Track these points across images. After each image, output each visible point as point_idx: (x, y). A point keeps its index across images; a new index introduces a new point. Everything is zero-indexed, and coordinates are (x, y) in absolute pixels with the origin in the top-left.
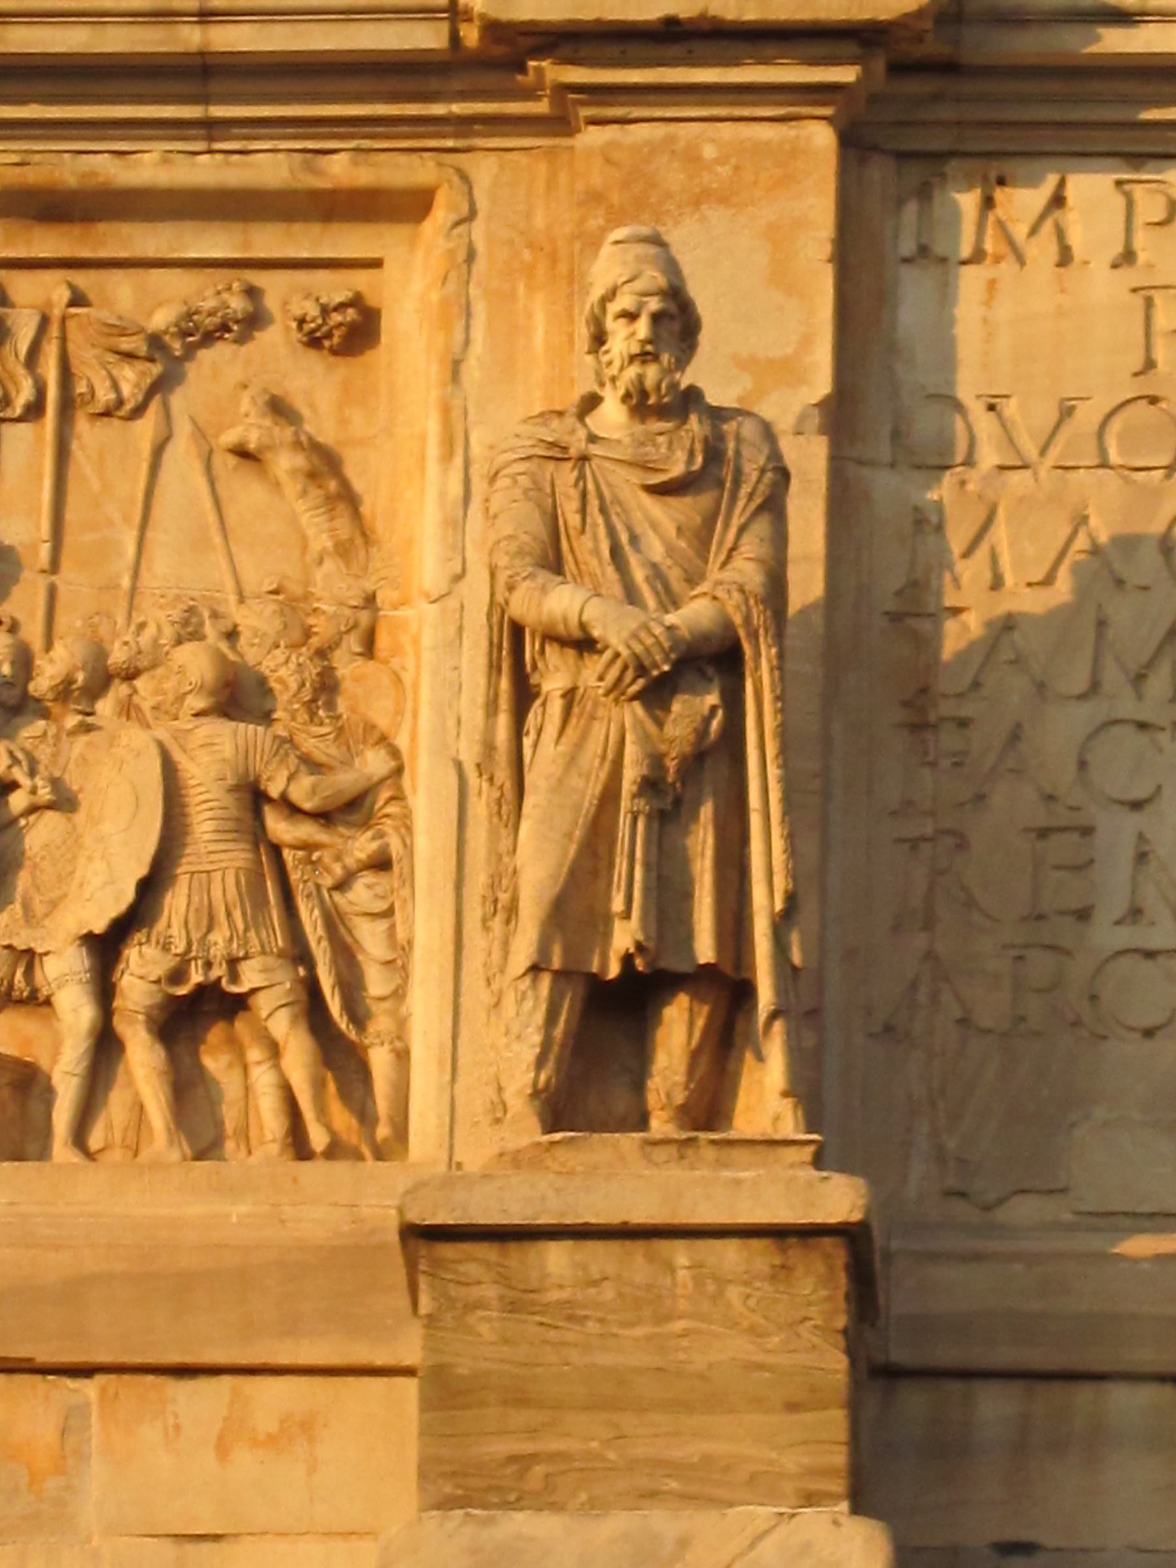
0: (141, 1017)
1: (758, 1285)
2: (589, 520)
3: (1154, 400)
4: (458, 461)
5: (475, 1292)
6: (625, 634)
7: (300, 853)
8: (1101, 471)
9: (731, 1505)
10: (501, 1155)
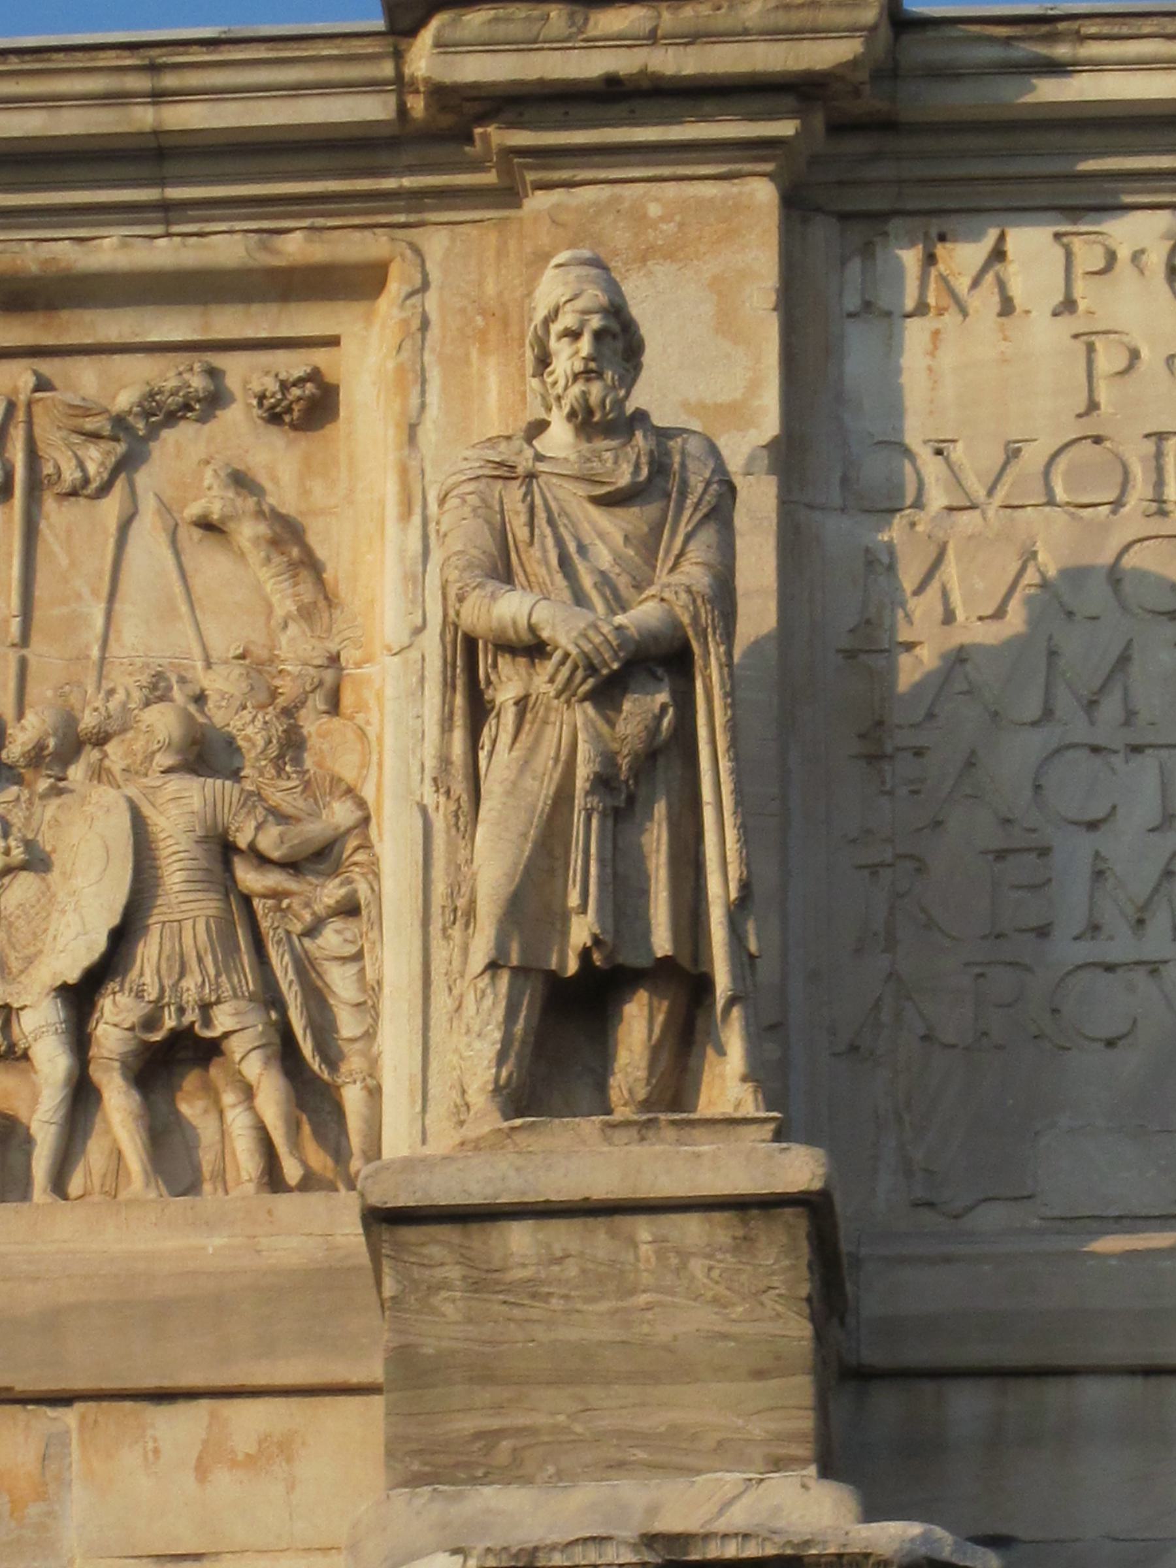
0: (117, 1065)
1: (719, 1256)
2: (537, 531)
3: (1098, 440)
4: (417, 519)
5: (439, 1273)
6: (574, 634)
7: (270, 902)
8: (1047, 509)
9: (699, 1472)
10: (462, 1144)
